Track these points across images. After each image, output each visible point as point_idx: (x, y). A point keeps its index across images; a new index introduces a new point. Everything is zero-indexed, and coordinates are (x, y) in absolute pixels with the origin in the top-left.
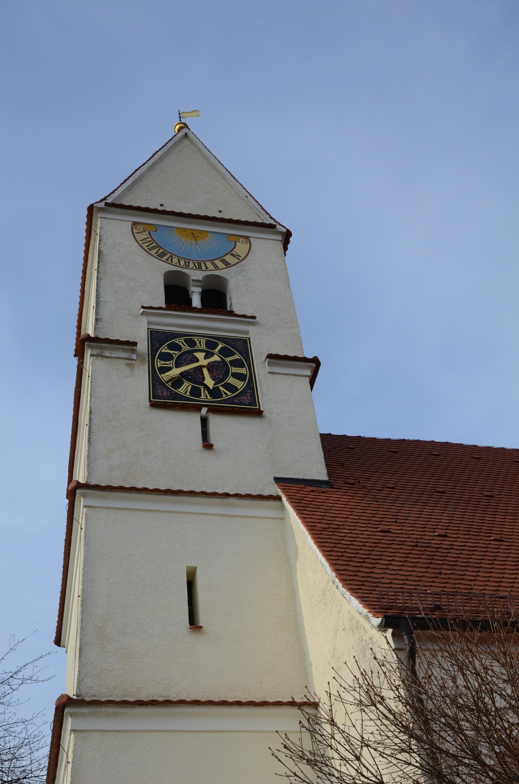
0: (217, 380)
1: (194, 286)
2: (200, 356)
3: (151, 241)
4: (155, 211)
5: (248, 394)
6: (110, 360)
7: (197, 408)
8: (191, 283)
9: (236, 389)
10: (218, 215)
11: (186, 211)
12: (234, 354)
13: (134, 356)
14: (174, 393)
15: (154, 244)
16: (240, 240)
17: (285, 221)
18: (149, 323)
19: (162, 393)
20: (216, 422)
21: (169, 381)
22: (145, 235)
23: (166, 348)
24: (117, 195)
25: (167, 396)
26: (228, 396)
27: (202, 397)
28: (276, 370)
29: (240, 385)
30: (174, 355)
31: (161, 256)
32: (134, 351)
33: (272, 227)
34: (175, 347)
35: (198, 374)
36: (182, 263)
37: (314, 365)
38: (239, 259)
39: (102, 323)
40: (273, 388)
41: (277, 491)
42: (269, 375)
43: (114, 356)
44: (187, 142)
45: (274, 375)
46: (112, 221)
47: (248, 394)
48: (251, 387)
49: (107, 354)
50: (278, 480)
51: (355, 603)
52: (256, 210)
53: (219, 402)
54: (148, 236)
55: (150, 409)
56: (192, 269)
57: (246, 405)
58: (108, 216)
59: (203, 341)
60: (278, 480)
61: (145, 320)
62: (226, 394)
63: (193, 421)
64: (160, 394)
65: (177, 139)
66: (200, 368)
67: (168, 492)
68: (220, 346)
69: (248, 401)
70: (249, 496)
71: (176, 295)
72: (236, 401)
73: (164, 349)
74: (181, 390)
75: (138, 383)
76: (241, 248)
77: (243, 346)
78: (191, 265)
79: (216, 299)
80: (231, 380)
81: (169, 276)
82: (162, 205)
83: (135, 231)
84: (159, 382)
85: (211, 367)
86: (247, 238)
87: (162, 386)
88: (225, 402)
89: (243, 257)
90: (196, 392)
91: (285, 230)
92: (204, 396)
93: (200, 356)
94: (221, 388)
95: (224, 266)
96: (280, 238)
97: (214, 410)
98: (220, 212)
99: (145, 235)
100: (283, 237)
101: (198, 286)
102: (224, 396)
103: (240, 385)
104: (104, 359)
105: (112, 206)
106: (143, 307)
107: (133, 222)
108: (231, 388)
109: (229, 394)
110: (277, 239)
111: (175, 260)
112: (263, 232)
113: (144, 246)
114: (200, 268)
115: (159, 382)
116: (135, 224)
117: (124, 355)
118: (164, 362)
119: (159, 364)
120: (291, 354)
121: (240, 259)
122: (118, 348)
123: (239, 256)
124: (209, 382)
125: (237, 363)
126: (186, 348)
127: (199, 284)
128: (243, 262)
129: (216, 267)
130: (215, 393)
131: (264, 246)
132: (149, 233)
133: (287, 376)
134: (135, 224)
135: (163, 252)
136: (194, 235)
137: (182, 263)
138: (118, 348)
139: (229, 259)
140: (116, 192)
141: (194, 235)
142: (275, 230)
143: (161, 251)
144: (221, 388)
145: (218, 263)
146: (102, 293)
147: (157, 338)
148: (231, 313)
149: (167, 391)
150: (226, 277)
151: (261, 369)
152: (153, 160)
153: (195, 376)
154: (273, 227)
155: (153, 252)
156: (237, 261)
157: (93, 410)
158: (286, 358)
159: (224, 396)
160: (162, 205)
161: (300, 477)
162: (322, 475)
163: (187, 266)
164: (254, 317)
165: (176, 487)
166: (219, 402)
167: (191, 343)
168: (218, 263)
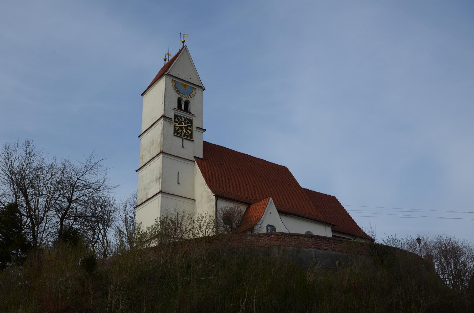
0: (186, 130)
2: (183, 123)
17: (205, 86)
20: (185, 141)
29: (190, 132)
31: (177, 92)
33: (202, 87)
34: (178, 120)
40: (196, 134)
41: (193, 159)
48: (192, 133)
50: (194, 157)
51: (210, 190)
57: (190, 137)
60: (194, 157)
67: (176, 156)
73: (176, 120)
77: (190, 121)
80: (188, 131)
85: (185, 127)
90: (181, 132)
93: (183, 123)
103: (190, 132)
108: (188, 133)
124: (184, 131)
125: (190, 126)
126: (180, 120)
130: (185, 133)
131: (199, 91)
134: (172, 80)
136: (185, 86)
139: (191, 95)
141: (185, 86)
147: (176, 116)
148: (190, 113)
151: (194, 129)
153: (181, 128)
162: (202, 158)
165: (178, 155)
167: (181, 119)
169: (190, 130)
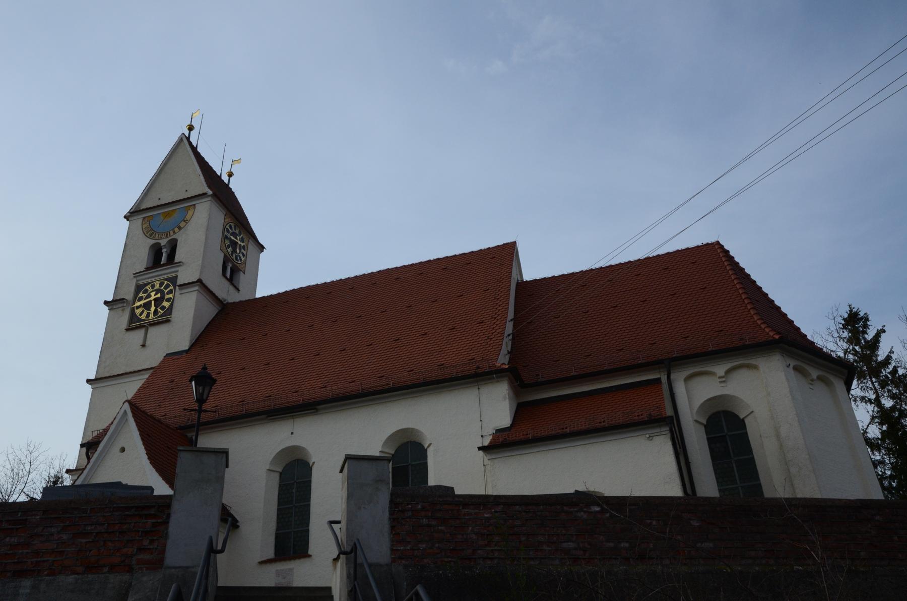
2: (153, 294)
28: (183, 291)
59: (158, 283)
66: (150, 301)
73: (141, 295)
85: (155, 300)
92: (152, 316)
108: (163, 308)
114: (166, 237)
116: (144, 218)
121: (186, 221)
129: (174, 233)
141: (167, 215)
145: (176, 230)
163: (161, 238)
169: (168, 300)
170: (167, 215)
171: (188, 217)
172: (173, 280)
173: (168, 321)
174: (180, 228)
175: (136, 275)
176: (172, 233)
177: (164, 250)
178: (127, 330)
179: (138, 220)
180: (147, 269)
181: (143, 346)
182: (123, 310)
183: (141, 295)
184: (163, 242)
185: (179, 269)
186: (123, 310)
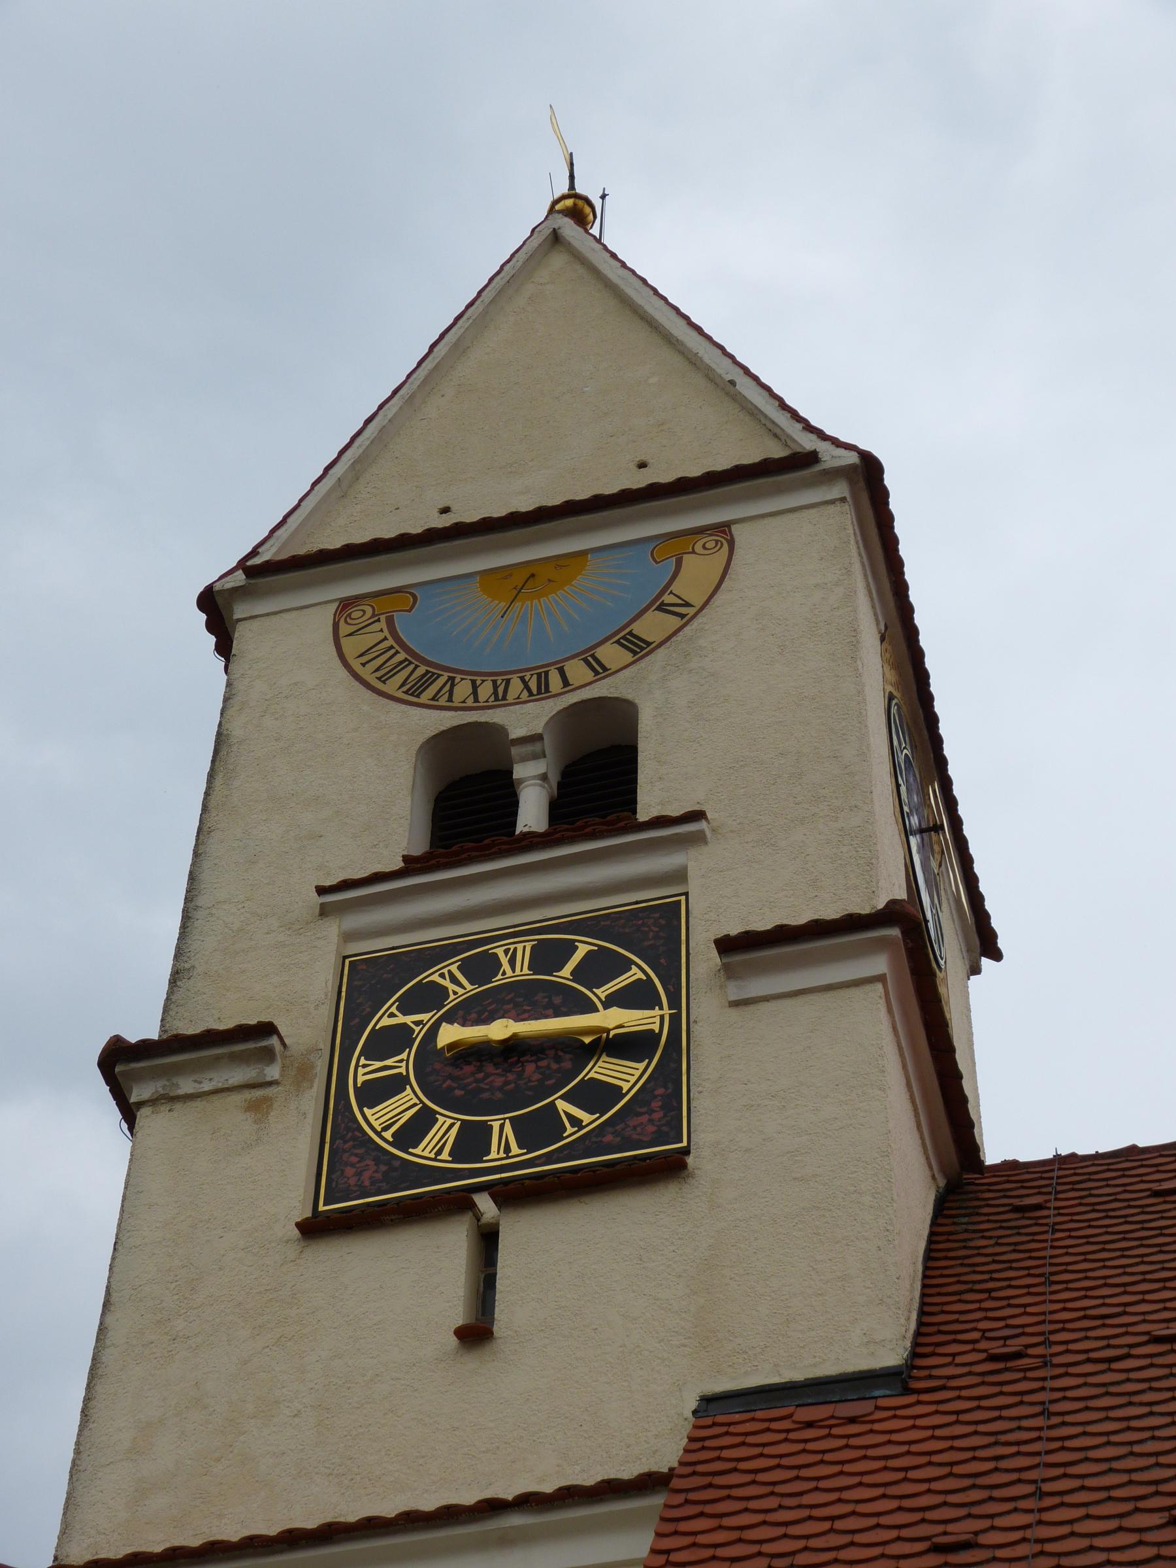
1: (524, 759)
3: (392, 647)
4: (431, 537)
5: (656, 1104)
6: (199, 1104)
7: (458, 1203)
8: (514, 751)
9: (615, 1093)
10: (639, 480)
11: (525, 504)
12: (626, 965)
13: (273, 1072)
14: (397, 1164)
15: (402, 656)
16: (698, 548)
18: (349, 937)
19: (359, 1174)
21: (386, 1129)
22: (376, 633)
23: (393, 1009)
24: (295, 526)
25: (372, 1183)
26: (581, 1128)
27: (493, 1155)
30: (417, 1029)
32: (268, 1055)
35: (487, 1076)
36: (485, 691)
37: (895, 932)
38: (682, 616)
39: (192, 981)
42: (734, 1013)
43: (207, 1086)
44: (558, 260)
45: (752, 1008)
46: (274, 619)
47: (656, 1104)
49: (186, 1086)
52: (763, 421)
53: (549, 1158)
54: (386, 633)
55: (303, 1244)
56: (518, 702)
58: (261, 607)
59: (524, 949)
61: (332, 929)
62: (576, 1122)
63: (447, 1248)
64: (352, 1181)
65: (520, 264)
68: (582, 950)
69: (651, 1128)
70: (569, 1496)
71: (467, 811)
72: (609, 1138)
73: (388, 1017)
74: (423, 1152)
75: (282, 1161)
76: (697, 572)
78: (516, 686)
79: (600, 782)
81: (441, 748)
82: (445, 510)
83: (344, 629)
84: (354, 1139)
86: (723, 529)
87: (360, 1151)
88: (589, 1143)
89: (698, 602)
91: (852, 458)
94: (562, 1105)
95: (628, 657)
96: (840, 489)
97: (518, 1194)
98: (642, 465)
99: (376, 633)
100: (852, 483)
101: (535, 757)
102: (570, 1130)
104: (178, 1106)
105: (263, 572)
106: (321, 891)
107: (341, 600)
109: (585, 1117)
110: (829, 497)
111: (463, 690)
112: (779, 491)
113: (366, 673)
114: (543, 690)
115: (354, 1139)
116: (346, 605)
117: (238, 1075)
118: (378, 1064)
119: (364, 1071)
120: (831, 912)
121: (684, 614)
122: (218, 1058)
123: (687, 604)
127: (537, 747)
128: (695, 624)
129: (600, 670)
132: (390, 622)
133: (800, 1000)
135: (427, 672)
137: (485, 691)
138: (218, 1058)
139: (651, 626)
140: (289, 520)
142: (817, 468)
143: (422, 669)
144: (562, 1105)
145: (611, 654)
146: (206, 876)
147: (367, 982)
149: (378, 1162)
150: (629, 697)
152: (429, 365)
154: (812, 458)
155: (392, 686)
156: (676, 622)
157: (115, 1297)
158: (783, 935)
159: (570, 1130)
160: (445, 510)
161: (798, 1376)
163: (500, 699)
164: (696, 816)
166: (549, 1158)
168: (611, 654)
170: (526, 582)
171: (689, 587)
172: (656, 931)
173: (673, 1167)
174: (638, 647)
175: (338, 895)
176: (578, 671)
177: (520, 771)
178: (315, 1228)
179: (296, 634)
180: (412, 866)
181: (476, 1334)
182: (259, 1108)
183: (388, 1017)
184: (524, 719)
185: (694, 861)
186: (259, 1108)
